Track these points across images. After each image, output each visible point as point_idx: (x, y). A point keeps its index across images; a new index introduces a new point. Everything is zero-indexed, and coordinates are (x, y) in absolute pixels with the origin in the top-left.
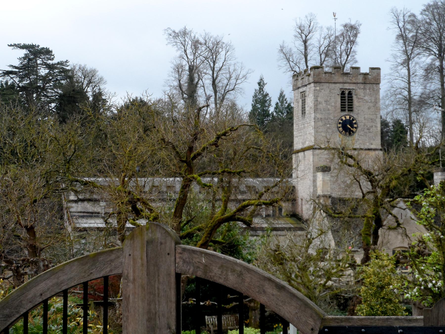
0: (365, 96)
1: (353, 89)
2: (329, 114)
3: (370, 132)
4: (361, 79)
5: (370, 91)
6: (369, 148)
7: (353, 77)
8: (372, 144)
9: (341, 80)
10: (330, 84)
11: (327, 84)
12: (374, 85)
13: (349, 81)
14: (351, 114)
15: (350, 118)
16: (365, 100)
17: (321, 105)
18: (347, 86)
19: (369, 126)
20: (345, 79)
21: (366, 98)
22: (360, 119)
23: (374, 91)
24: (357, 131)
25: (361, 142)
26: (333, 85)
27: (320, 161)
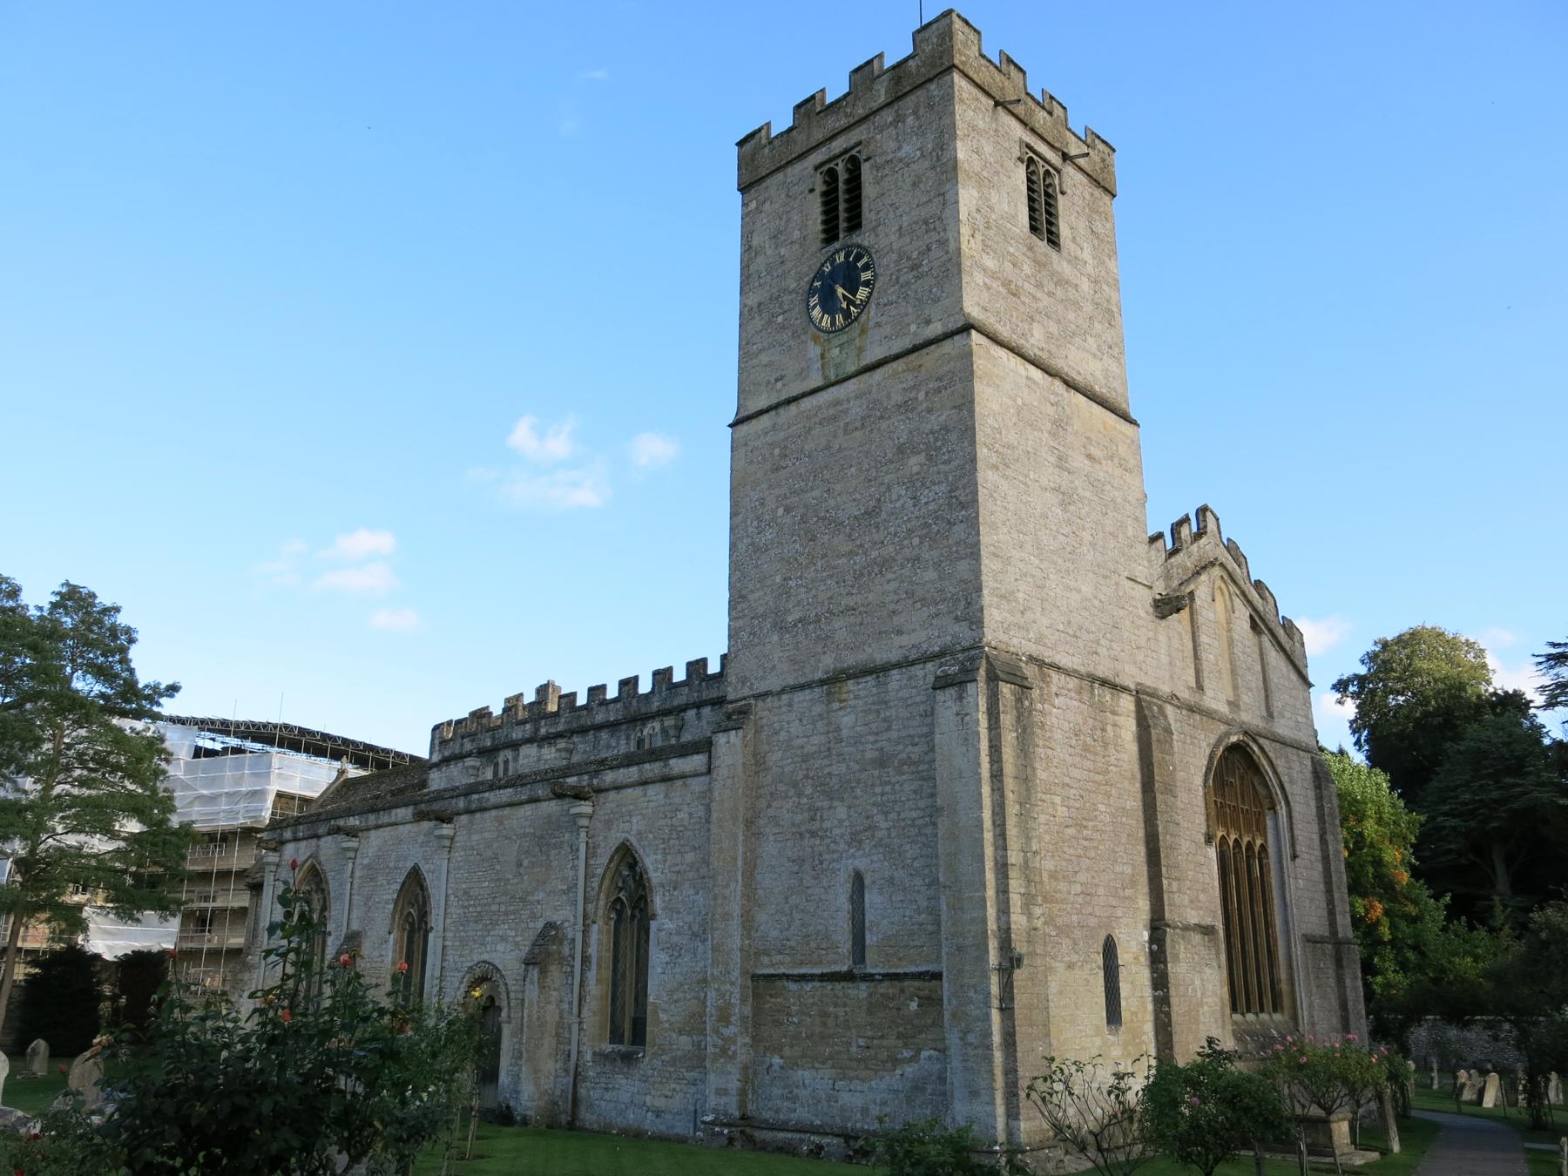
0: (900, 148)
1: (859, 143)
2: (783, 276)
3: (917, 278)
4: (883, 91)
5: (918, 118)
6: (919, 341)
7: (857, 98)
8: (928, 322)
9: (818, 135)
10: (789, 170)
11: (780, 176)
12: (932, 86)
13: (844, 122)
14: (857, 239)
15: (847, 256)
16: (901, 160)
17: (760, 259)
18: (838, 145)
19: (915, 255)
20: (834, 122)
21: (906, 149)
22: (883, 242)
23: (931, 107)
24: (875, 294)
25: (888, 330)
26: (797, 168)
27: (752, 462)
